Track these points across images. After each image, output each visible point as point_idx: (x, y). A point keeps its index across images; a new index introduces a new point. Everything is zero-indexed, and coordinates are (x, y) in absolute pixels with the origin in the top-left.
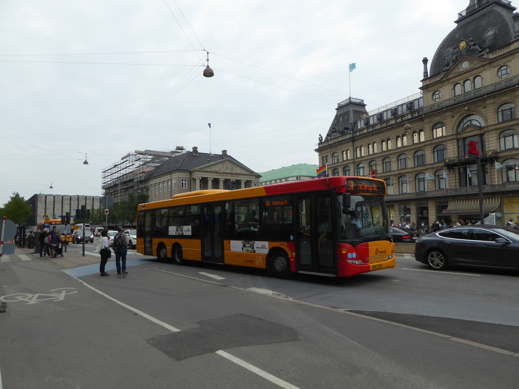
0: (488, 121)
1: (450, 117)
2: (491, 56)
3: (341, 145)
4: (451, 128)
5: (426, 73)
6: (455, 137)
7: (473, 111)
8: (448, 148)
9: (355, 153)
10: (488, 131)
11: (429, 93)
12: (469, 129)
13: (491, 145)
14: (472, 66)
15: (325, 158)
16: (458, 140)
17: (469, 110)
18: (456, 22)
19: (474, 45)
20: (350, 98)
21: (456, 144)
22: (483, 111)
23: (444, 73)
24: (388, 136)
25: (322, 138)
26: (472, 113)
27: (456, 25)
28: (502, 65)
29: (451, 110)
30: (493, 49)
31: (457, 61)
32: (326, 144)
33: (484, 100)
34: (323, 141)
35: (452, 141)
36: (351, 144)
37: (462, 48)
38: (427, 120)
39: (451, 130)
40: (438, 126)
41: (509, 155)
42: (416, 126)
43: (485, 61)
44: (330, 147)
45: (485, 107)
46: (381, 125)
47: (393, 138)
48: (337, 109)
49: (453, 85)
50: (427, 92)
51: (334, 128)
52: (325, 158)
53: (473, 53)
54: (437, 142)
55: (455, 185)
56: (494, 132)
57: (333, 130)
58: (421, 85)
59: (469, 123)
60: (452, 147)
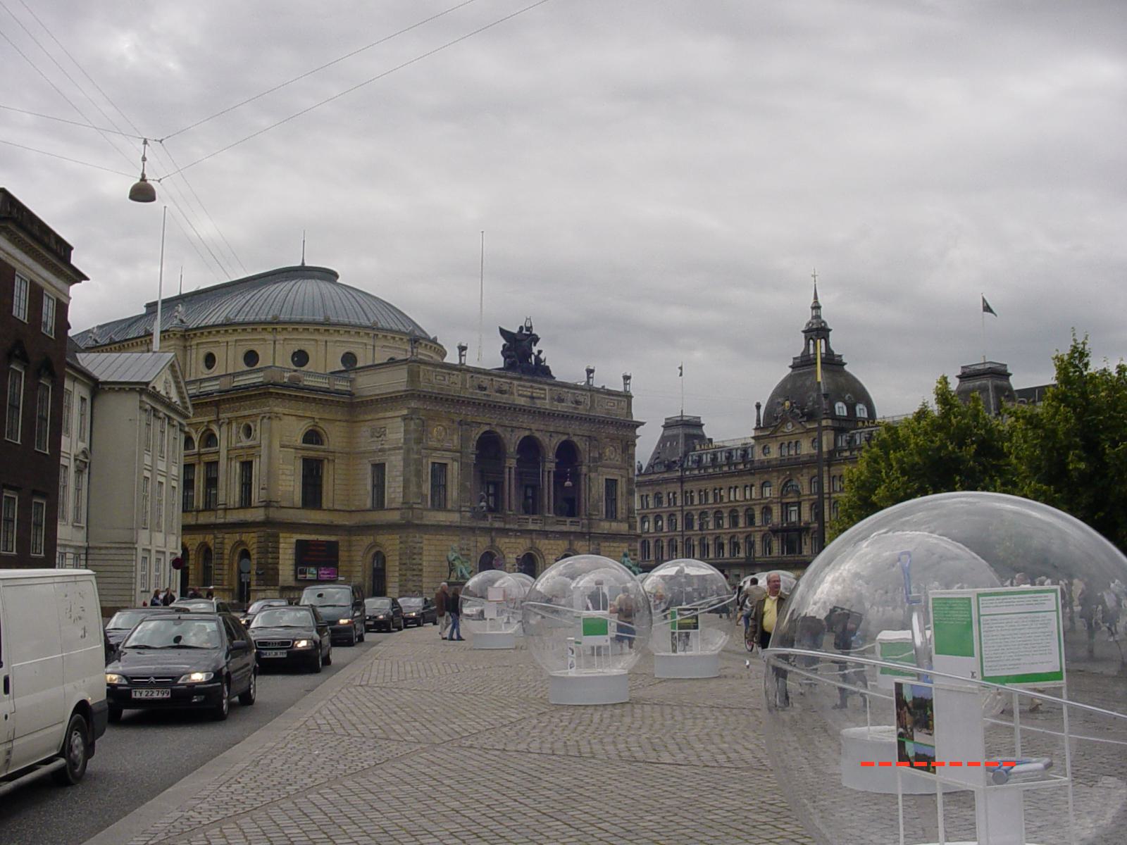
2: (808, 427)
3: (667, 483)
5: (758, 420)
6: (779, 500)
10: (804, 500)
12: (790, 495)
15: (644, 498)
16: (782, 504)
17: (790, 474)
18: (790, 367)
19: (797, 408)
20: (682, 416)
21: (780, 507)
23: (772, 429)
25: (641, 467)
27: (790, 370)
29: (778, 471)
30: (811, 416)
31: (784, 421)
32: (646, 478)
33: (802, 469)
34: (643, 471)
36: (679, 484)
38: (758, 476)
42: (748, 480)
44: (652, 483)
45: (802, 475)
48: (663, 426)
51: (658, 458)
52: (644, 498)
57: (657, 461)
58: (753, 434)
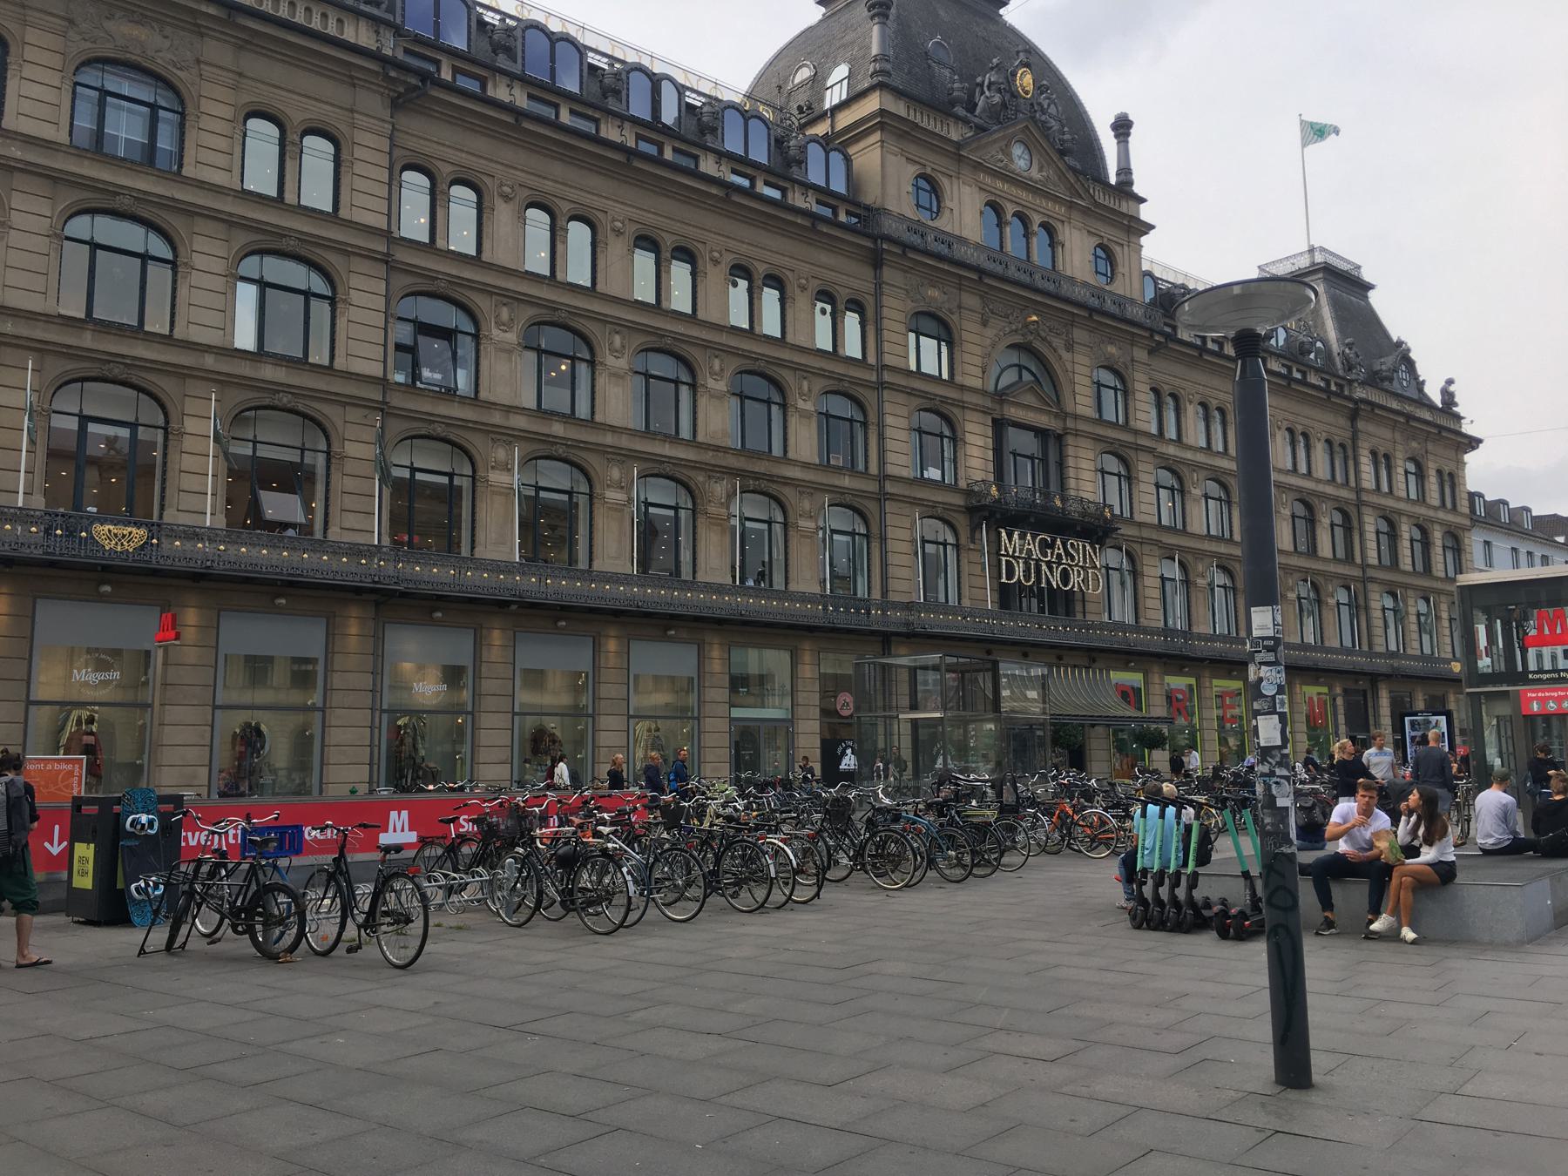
24: (785, 261)
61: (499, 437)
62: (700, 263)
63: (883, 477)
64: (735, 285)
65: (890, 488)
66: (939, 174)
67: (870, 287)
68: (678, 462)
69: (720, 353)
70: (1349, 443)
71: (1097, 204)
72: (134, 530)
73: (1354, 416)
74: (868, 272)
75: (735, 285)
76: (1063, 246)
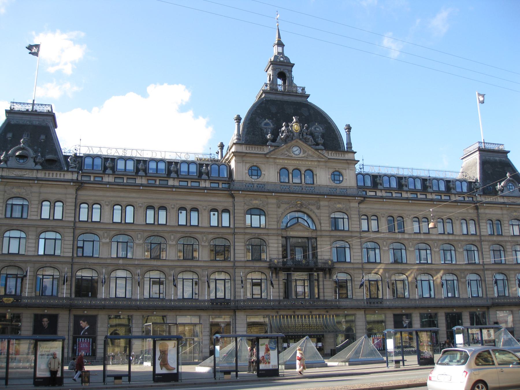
0: (322, 225)
1: (275, 206)
4: (276, 220)
6: (279, 232)
7: (306, 208)
8: (271, 245)
9: (78, 210)
10: (321, 236)
11: (244, 163)
13: (324, 254)
14: (306, 156)
22: (316, 211)
26: (303, 210)
28: (337, 170)
35: (276, 238)
37: (297, 131)
39: (276, 223)
40: (254, 211)
41: (343, 268)
43: (323, 158)
46: (148, 180)
47: (173, 208)
49: (279, 167)
50: (243, 162)
53: (306, 141)
54: (255, 233)
55: (278, 295)
56: (328, 239)
59: (295, 221)
60: (276, 245)
61: (171, 268)
62: (168, 209)
63: (235, 261)
64: (181, 213)
65: (237, 264)
66: (260, 164)
67: (231, 204)
68: (159, 266)
69: (174, 234)
70: (476, 219)
71: (329, 159)
72: (11, 299)
73: (477, 208)
74: (231, 200)
75: (181, 213)
76: (316, 175)
